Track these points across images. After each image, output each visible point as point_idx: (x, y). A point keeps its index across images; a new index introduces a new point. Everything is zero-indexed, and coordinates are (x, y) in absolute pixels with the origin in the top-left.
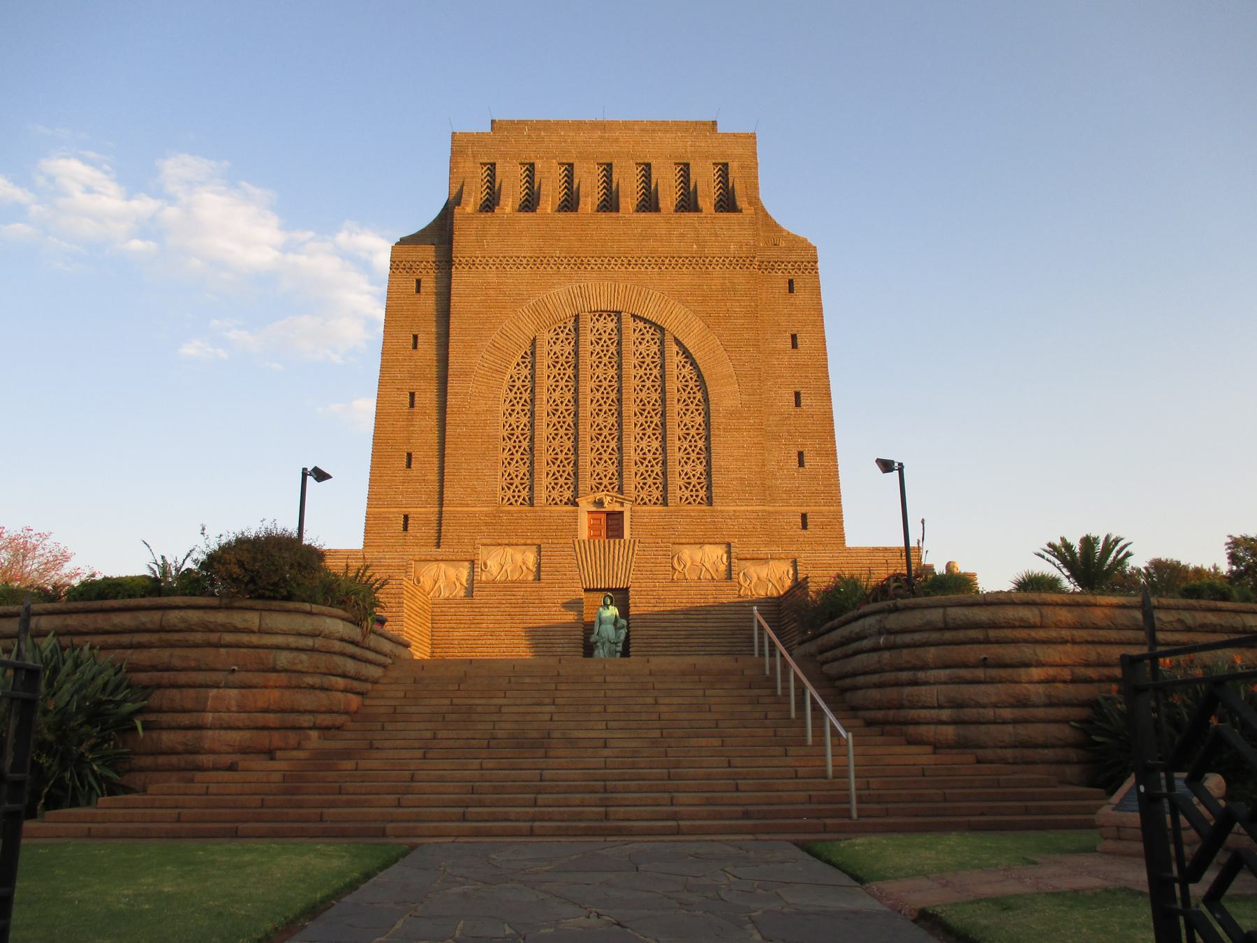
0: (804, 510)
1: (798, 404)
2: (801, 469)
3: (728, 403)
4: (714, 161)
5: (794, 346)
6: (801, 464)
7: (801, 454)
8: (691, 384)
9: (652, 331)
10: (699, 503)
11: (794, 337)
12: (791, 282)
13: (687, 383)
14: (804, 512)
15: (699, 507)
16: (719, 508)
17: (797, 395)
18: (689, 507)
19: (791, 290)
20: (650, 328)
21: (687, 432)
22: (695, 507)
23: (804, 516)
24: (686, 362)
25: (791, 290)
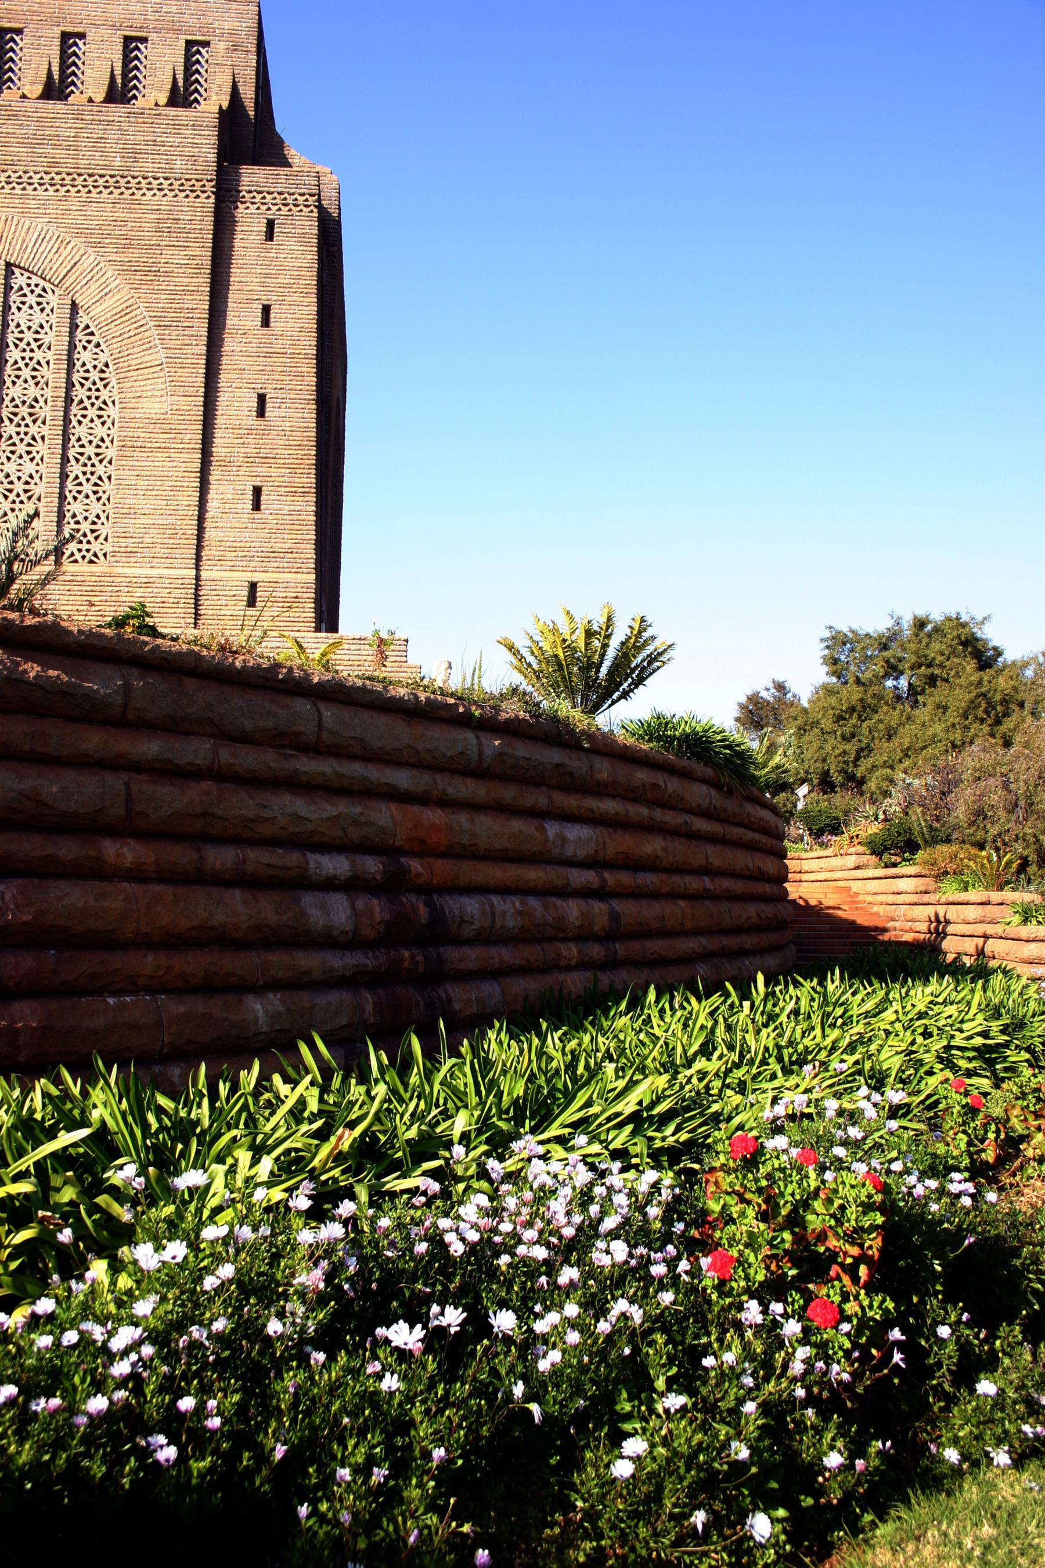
0: (255, 577)
1: (261, 412)
2: (257, 515)
3: (153, 407)
4: (190, 38)
5: (266, 322)
6: (257, 506)
7: (257, 491)
8: (94, 375)
9: (38, 291)
10: (91, 562)
11: (266, 310)
12: (270, 224)
13: (86, 375)
14: (254, 580)
15: (93, 568)
16: (120, 570)
17: (262, 399)
18: (74, 568)
19: (270, 235)
20: (37, 285)
21: (81, 450)
22: (83, 567)
23: (253, 586)
24: (89, 342)
25: (270, 235)
